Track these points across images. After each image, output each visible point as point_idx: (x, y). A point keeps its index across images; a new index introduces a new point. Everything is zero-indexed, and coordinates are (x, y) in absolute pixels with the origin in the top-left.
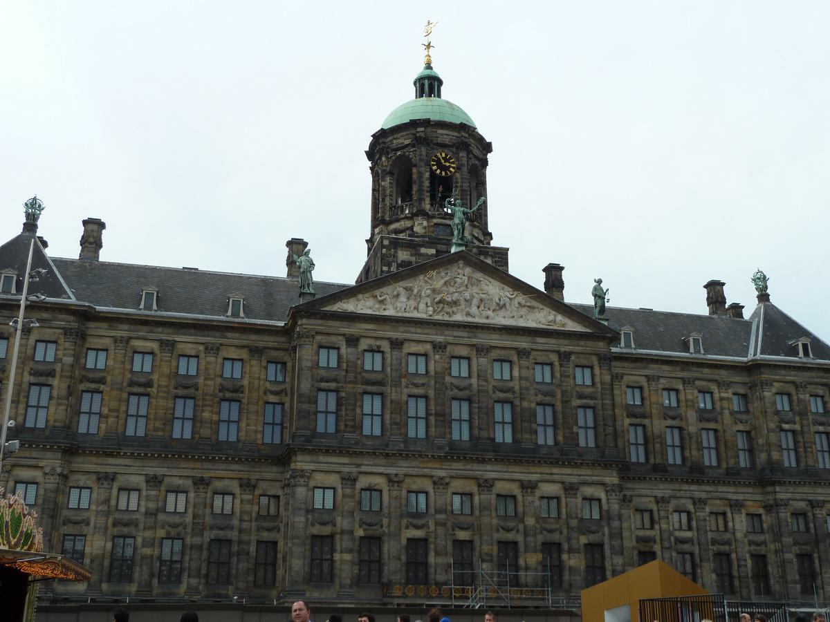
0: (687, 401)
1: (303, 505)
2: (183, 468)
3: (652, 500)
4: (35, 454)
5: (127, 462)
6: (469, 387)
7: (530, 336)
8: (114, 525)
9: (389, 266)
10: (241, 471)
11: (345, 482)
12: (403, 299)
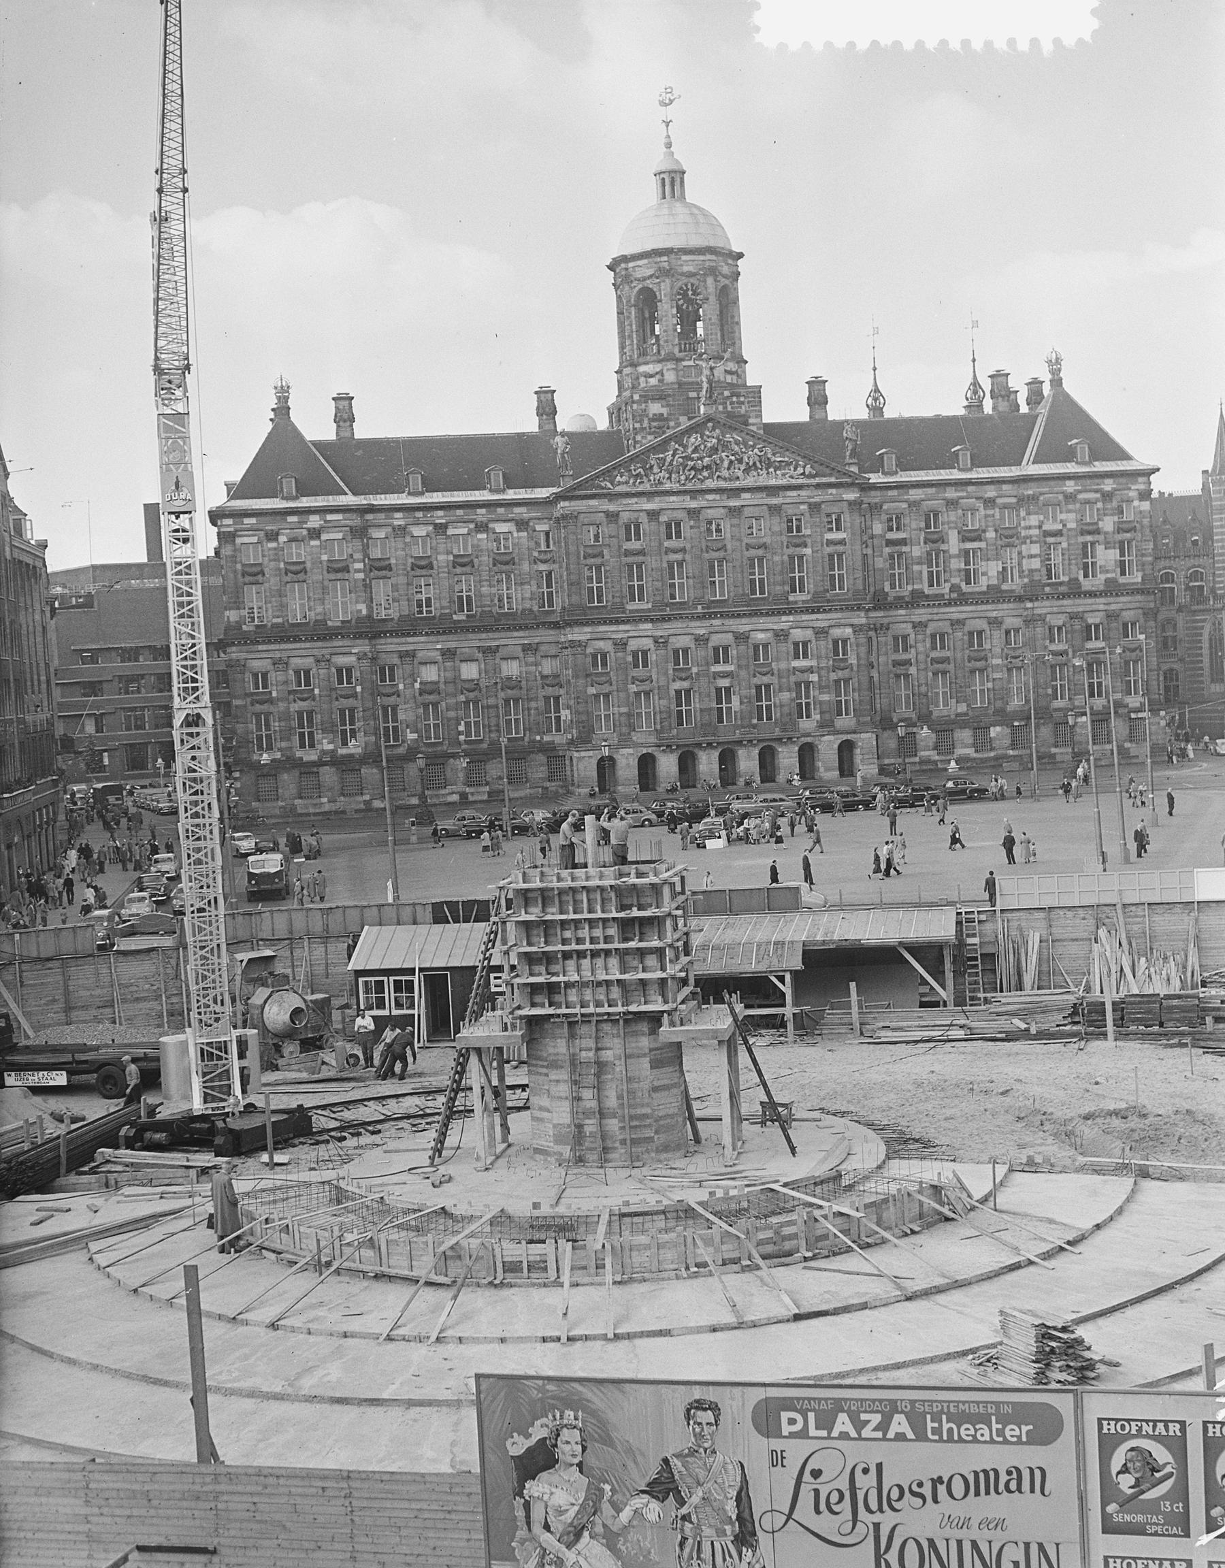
0: (948, 523)
3: (910, 626)
4: (347, 642)
5: (422, 639)
6: (724, 548)
8: (420, 694)
9: (641, 422)
12: (656, 470)
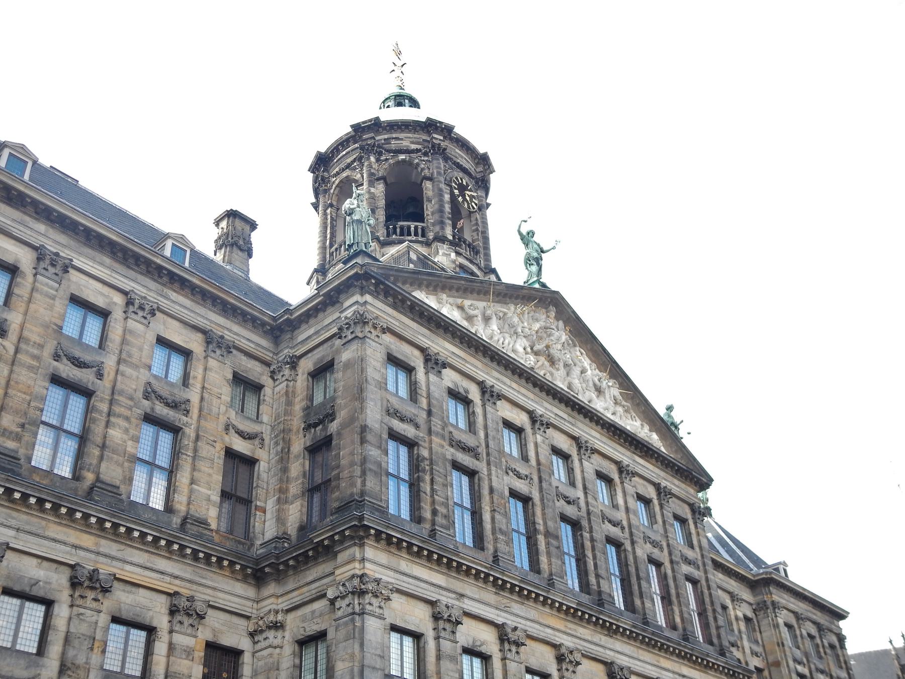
1: (378, 660)
2: (55, 540)
7: (629, 450)
10: (176, 577)
11: (441, 624)
12: (494, 326)
